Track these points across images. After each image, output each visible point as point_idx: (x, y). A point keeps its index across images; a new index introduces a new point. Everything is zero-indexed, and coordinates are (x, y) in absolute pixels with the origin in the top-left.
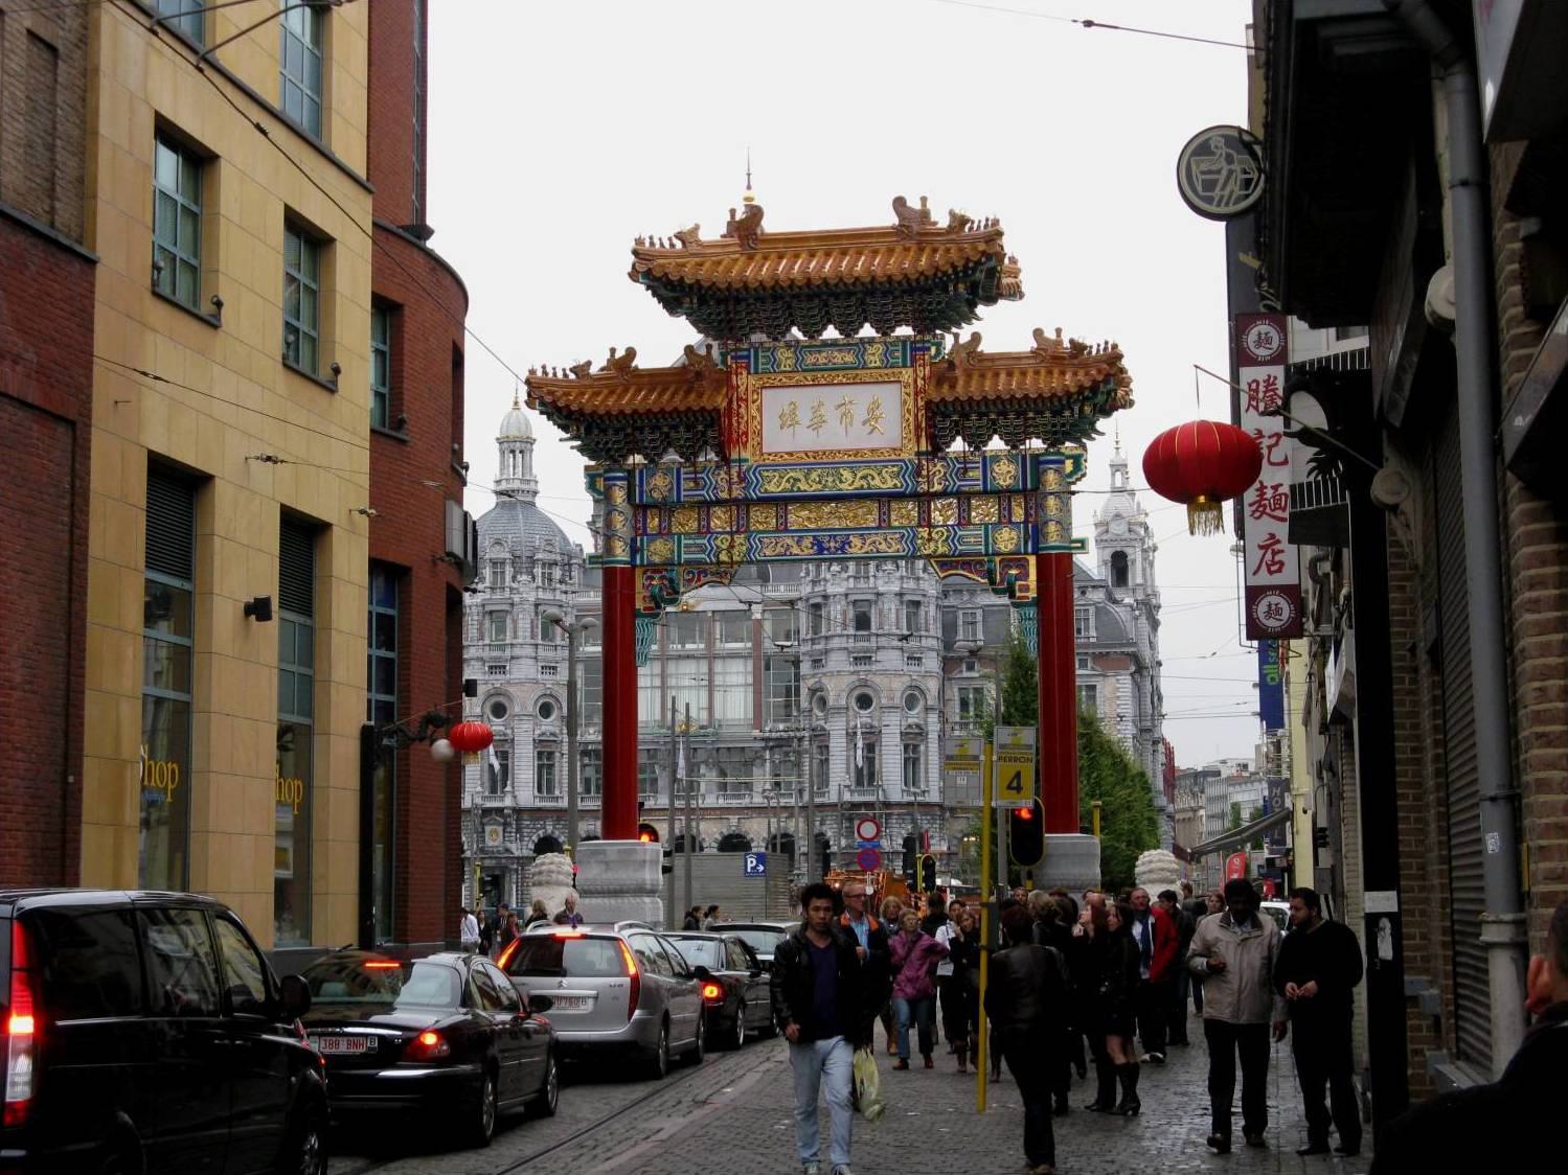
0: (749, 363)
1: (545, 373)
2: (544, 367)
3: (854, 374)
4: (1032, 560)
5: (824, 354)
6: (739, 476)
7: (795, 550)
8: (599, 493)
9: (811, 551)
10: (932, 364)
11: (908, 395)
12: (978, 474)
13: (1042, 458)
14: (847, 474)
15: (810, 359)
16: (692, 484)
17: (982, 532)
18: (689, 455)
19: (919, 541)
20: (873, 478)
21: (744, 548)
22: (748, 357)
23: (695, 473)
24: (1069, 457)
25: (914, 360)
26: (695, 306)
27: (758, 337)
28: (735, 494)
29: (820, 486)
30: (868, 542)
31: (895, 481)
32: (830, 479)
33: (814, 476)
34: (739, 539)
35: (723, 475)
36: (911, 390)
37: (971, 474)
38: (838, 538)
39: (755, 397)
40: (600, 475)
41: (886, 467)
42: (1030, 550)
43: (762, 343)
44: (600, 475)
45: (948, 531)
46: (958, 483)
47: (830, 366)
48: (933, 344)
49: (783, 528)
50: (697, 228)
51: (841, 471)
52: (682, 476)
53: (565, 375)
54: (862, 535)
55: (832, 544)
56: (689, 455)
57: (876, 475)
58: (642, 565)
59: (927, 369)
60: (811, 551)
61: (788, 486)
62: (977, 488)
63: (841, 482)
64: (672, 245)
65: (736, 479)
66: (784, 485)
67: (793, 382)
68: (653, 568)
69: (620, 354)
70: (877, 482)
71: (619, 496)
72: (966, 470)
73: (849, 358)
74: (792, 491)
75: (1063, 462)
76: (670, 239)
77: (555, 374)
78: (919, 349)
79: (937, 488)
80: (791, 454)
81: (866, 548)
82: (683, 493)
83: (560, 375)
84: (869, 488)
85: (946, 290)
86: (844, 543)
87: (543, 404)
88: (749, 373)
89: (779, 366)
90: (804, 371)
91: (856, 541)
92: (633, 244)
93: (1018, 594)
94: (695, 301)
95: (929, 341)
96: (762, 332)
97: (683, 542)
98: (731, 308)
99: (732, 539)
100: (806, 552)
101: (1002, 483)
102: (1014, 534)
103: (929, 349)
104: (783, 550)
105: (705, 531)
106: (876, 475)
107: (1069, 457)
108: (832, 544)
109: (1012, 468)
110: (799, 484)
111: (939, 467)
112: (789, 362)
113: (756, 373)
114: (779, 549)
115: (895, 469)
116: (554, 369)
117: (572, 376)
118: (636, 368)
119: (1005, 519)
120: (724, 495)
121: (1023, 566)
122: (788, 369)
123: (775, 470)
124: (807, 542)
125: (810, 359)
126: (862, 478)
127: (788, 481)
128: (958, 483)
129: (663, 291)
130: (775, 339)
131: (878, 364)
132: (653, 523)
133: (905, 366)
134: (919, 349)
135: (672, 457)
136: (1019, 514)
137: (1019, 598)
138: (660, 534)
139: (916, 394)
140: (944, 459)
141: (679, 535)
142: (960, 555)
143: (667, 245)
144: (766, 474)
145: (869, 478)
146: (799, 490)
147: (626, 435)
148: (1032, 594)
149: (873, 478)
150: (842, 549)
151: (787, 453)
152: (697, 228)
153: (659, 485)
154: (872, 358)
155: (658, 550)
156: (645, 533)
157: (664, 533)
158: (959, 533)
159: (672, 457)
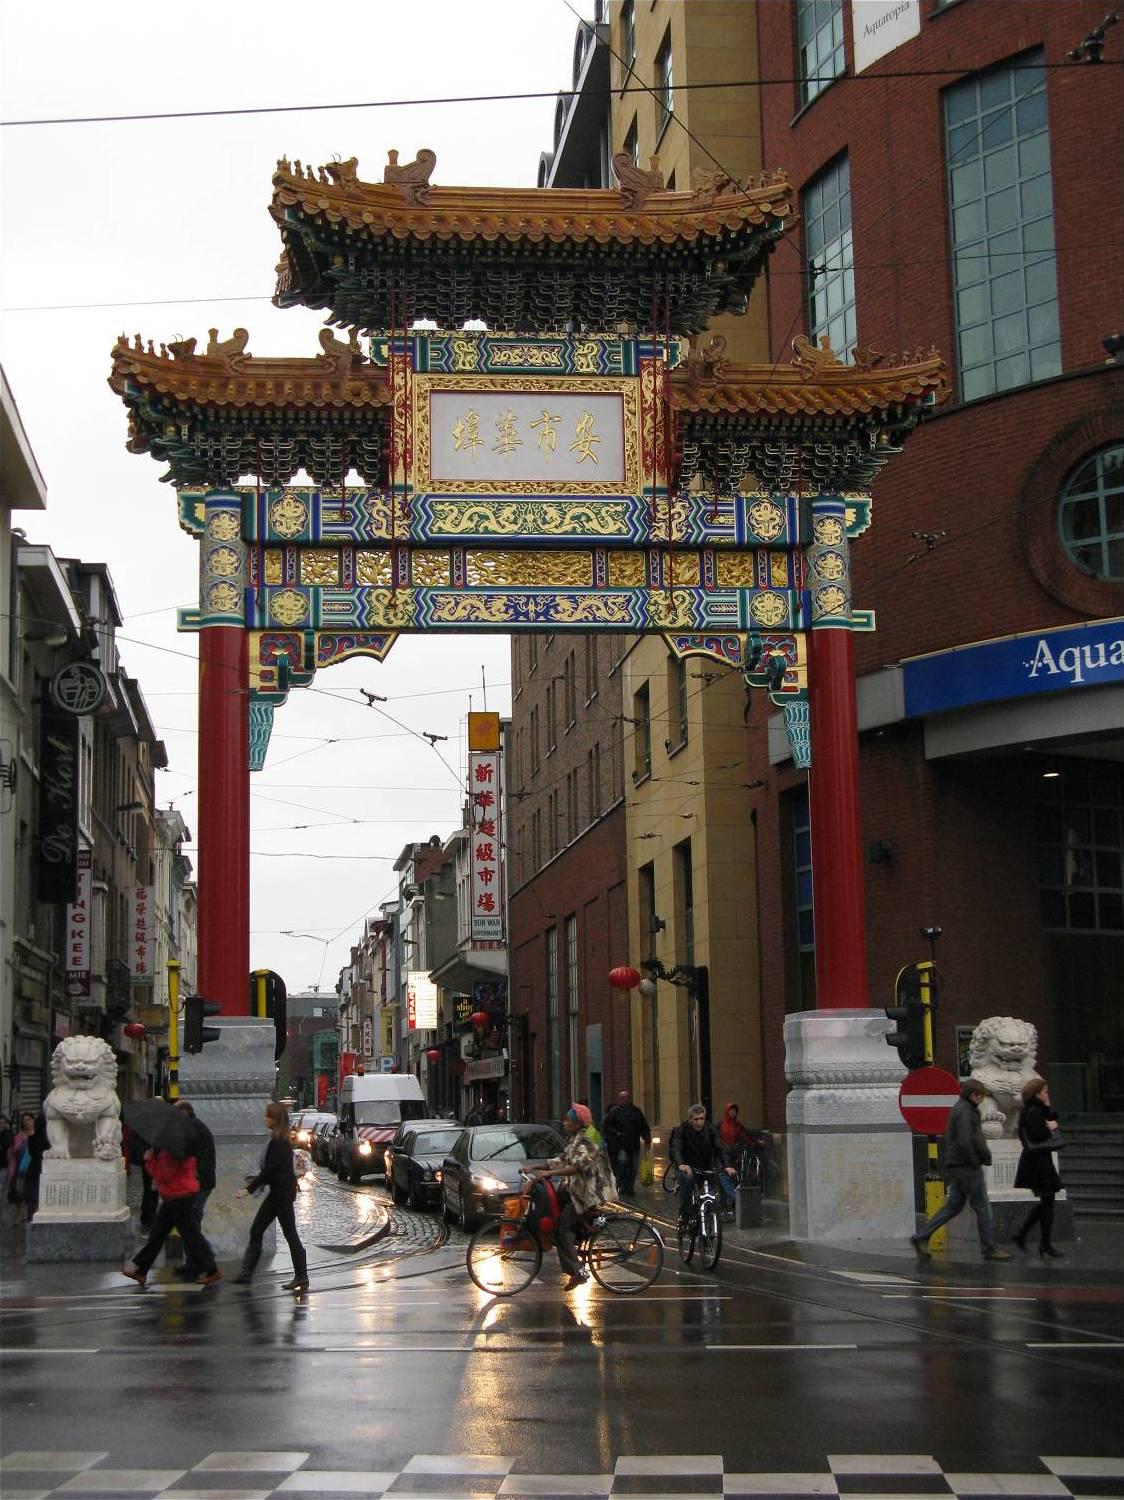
0: (413, 358)
1: (139, 346)
2: (138, 337)
3: (554, 380)
4: (801, 639)
5: (517, 351)
6: (402, 509)
7: (484, 614)
8: (199, 523)
9: (506, 617)
10: (667, 373)
11: (634, 414)
12: (732, 520)
13: (814, 505)
14: (552, 513)
15: (499, 358)
16: (335, 517)
17: (737, 599)
18: (328, 476)
19: (652, 608)
20: (589, 519)
21: (410, 608)
22: (413, 349)
23: (343, 501)
24: (850, 505)
25: (640, 367)
26: (352, 268)
27: (425, 325)
28: (398, 533)
29: (515, 528)
30: (582, 605)
31: (619, 525)
32: (530, 517)
33: (507, 512)
34: (404, 595)
35: (380, 506)
36: (635, 407)
37: (722, 519)
38: (539, 600)
39: (422, 403)
40: (200, 500)
41: (607, 504)
42: (801, 625)
43: (433, 332)
44: (200, 500)
45: (691, 594)
46: (705, 531)
47: (526, 366)
48: (666, 347)
49: (458, 583)
50: (354, 163)
51: (544, 506)
52: (322, 505)
53: (164, 354)
54: (570, 597)
55: (532, 607)
56: (328, 476)
57: (593, 516)
58: (262, 628)
59: (660, 379)
60: (506, 617)
61: (472, 525)
62: (728, 540)
63: (545, 522)
64: (324, 178)
65: (398, 513)
66: (466, 524)
67: (475, 387)
68: (275, 634)
69: (406, 158)
70: (594, 525)
71: (227, 526)
72: (715, 514)
73: (554, 359)
74: (477, 532)
75: (842, 510)
76: (321, 170)
77: (151, 349)
78: (647, 352)
79: (676, 536)
80: (470, 483)
81: (578, 615)
82: (322, 528)
83: (158, 352)
84: (583, 533)
85: (701, 270)
86: (548, 607)
87: (137, 386)
88: (414, 371)
89: (455, 363)
90: (491, 372)
91: (565, 604)
92: (274, 169)
93: (784, 684)
94: (352, 261)
95: (661, 343)
96: (430, 319)
97: (322, 597)
98: (402, 272)
99: (394, 595)
100: (499, 617)
101: (762, 533)
102: (779, 603)
103: (660, 353)
104: (465, 613)
105: (347, 581)
106: (593, 516)
107: (850, 505)
108: (532, 607)
109: (776, 514)
110: (486, 523)
111: (678, 508)
112: (469, 358)
113: (424, 371)
114: (461, 613)
115: (619, 508)
116: (150, 342)
117: (172, 357)
118: (249, 357)
119: (763, 584)
120: (382, 533)
121: (790, 647)
122: (468, 368)
123: (452, 503)
124: (498, 604)
125: (499, 358)
126: (572, 518)
127: (470, 519)
128: (705, 531)
129: (147, 411)
130: (451, 328)
131: (592, 368)
132: (273, 570)
133: (628, 374)
134: (647, 352)
135: (302, 479)
136: (780, 574)
137: (787, 689)
138: (284, 585)
139: (644, 410)
140: (686, 497)
141: (316, 588)
142: (706, 629)
143: (317, 175)
144: (440, 507)
145: (583, 519)
146: (486, 530)
147: (245, 443)
148: (802, 682)
149: (589, 519)
150: (546, 613)
151: (467, 482)
152: (354, 163)
153: (287, 519)
154: (583, 360)
155: (287, 608)
156: (261, 584)
157: (291, 582)
158: (706, 599)
159: (302, 479)
